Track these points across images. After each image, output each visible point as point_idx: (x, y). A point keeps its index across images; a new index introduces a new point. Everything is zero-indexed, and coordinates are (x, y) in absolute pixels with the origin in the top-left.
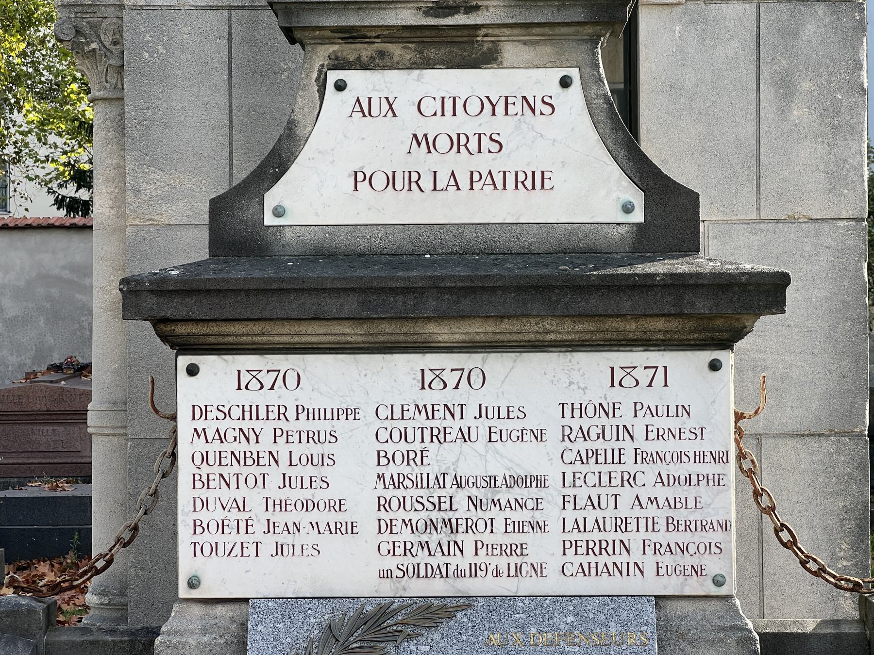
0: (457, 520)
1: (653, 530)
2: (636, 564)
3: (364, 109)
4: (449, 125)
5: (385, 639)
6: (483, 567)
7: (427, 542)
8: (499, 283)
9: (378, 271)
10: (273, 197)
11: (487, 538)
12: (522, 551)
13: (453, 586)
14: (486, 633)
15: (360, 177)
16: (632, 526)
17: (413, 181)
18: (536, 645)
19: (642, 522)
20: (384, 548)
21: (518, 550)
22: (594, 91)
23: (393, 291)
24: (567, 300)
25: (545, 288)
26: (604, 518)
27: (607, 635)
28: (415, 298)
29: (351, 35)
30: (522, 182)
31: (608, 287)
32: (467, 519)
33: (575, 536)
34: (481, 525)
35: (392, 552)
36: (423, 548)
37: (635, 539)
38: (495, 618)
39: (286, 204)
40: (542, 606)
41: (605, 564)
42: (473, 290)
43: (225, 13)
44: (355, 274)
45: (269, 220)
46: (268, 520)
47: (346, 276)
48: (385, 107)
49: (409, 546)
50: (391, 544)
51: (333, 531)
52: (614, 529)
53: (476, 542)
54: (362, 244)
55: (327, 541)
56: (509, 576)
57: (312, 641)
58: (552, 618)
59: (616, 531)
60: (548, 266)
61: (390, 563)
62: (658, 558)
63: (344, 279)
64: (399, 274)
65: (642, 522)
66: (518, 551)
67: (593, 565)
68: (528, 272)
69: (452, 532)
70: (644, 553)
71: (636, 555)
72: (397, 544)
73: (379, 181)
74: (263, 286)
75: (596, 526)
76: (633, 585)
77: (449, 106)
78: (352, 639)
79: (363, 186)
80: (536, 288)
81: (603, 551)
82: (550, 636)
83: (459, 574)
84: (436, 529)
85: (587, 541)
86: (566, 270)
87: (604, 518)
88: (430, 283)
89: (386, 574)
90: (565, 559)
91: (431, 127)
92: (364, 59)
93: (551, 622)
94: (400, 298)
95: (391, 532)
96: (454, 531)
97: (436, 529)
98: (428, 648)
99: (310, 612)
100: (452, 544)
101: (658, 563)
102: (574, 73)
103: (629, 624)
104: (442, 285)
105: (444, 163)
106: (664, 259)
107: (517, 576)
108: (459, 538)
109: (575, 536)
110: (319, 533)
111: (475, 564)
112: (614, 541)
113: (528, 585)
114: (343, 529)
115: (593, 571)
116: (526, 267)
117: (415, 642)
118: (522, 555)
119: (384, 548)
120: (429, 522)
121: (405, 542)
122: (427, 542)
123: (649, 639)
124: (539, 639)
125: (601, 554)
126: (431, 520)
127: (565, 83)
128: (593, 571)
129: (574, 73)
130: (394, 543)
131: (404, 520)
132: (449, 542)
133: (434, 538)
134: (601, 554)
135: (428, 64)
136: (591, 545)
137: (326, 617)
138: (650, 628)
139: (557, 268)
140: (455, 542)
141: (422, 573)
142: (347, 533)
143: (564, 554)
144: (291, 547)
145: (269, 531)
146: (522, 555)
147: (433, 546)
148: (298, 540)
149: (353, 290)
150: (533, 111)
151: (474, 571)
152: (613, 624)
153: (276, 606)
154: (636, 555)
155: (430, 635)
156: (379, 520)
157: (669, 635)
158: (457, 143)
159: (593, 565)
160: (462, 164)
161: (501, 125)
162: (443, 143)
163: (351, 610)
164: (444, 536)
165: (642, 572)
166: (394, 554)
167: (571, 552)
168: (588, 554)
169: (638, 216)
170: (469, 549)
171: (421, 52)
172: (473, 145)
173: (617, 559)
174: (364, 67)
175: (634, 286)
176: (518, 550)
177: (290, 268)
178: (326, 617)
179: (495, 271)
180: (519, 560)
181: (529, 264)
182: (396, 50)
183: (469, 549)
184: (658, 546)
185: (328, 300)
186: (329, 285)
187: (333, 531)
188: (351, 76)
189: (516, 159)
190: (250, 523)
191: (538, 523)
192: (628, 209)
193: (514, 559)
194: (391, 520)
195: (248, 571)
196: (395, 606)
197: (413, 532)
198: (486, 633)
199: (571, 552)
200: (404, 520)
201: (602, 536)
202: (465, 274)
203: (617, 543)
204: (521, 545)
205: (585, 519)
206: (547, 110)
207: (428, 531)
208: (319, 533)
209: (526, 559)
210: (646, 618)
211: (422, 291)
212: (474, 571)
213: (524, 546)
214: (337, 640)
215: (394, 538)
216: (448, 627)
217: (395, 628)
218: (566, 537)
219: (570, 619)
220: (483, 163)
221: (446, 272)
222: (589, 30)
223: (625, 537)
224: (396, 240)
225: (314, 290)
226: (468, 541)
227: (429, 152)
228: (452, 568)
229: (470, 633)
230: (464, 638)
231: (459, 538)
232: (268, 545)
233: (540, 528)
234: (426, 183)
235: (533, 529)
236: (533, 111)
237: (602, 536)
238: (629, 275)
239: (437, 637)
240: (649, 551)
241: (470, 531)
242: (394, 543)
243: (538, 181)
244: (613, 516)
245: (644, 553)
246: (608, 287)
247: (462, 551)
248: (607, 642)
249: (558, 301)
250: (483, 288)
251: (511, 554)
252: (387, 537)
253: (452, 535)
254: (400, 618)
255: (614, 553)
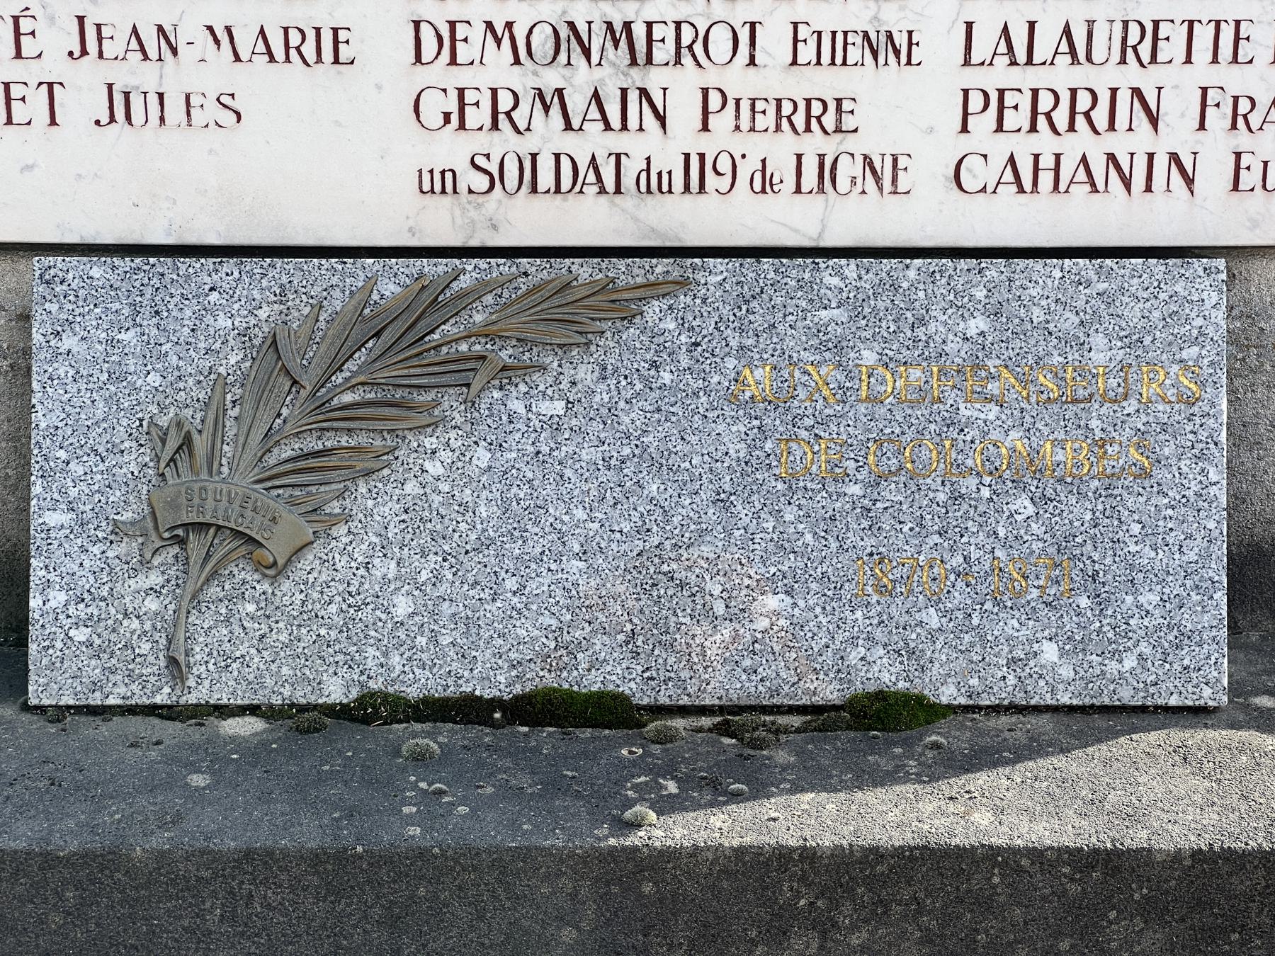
0: (649, 25)
1: (1235, 59)
2: (1175, 158)
5: (433, 380)
6: (724, 165)
7: (559, 92)
11: (738, 81)
12: (839, 121)
13: (636, 220)
14: (731, 363)
16: (1173, 49)
18: (875, 400)
19: (1204, 36)
20: (434, 106)
21: (830, 115)
26: (1090, 23)
27: (1081, 371)
32: (678, 25)
33: (1000, 75)
34: (720, 42)
35: (455, 118)
36: (546, 108)
37: (1176, 86)
38: (759, 321)
40: (895, 287)
41: (1084, 160)
46: (81, 19)
49: (505, 102)
50: (453, 95)
51: (279, 53)
52: (1116, 56)
53: (705, 92)
55: (258, 83)
56: (798, 190)
57: (222, 383)
58: (922, 322)
59: (1123, 61)
61: (452, 150)
62: (1242, 139)
65: (1204, 36)
66: (829, 121)
67: (1047, 162)
69: (634, 62)
70: (1202, 127)
71: (1178, 133)
72: (470, 97)
75: (1064, 47)
76: (1162, 217)
78: (339, 378)
81: (1080, 120)
82: (916, 373)
83: (653, 183)
84: (587, 53)
85: (1035, 92)
87: (1090, 23)
89: (440, 183)
90: (966, 144)
93: (920, 332)
95: (453, 61)
96: (642, 58)
97: (587, 53)
98: (559, 407)
99: (214, 296)
100: (633, 96)
101: (1238, 155)
103: (1147, 340)
107: (821, 190)
108: (655, 80)
109: (1000, 75)
110: (237, 58)
111: (702, 156)
112: (1114, 91)
113: (854, 218)
114: (309, 50)
115: (1046, 179)
117: (523, 388)
118: (838, 130)
119: (434, 106)
120: (564, 32)
121: (494, 92)
122: (559, 92)
123: (1203, 385)
124: (883, 382)
125: (1072, 128)
126: (571, 25)
128: (1046, 179)
130: (461, 92)
131: (489, 25)
132: (624, 91)
133: (579, 80)
134: (1072, 128)
136: (1045, 102)
137: (263, 314)
138: (1209, 353)
140: (644, 92)
141: (546, 179)
142: (319, 59)
143: (965, 129)
144: (153, 100)
145: (84, 52)
146: (838, 130)
147: (577, 102)
148: (176, 78)
151: (696, 175)
152: (1099, 340)
153: (114, 279)
154: (1178, 133)
155: (568, 371)
156: (417, 24)
157: (1253, 361)
159: (1047, 162)
163: (337, 293)
164: (610, 74)
165: (1189, 182)
166: (462, 126)
167: (983, 123)
168: (1033, 129)
170: (684, 111)
173: (1120, 144)
176: (830, 115)
178: (263, 314)
180: (830, 146)
183: (684, 111)
184: (1244, 106)
187: (279, 53)
190: (25, 25)
191: (890, 36)
193: (814, 144)
194: (452, 25)
195: (28, 168)
196: (464, 282)
197: (517, 61)
198: (731, 363)
199: (983, 123)
200: (489, 25)
201: (1081, 76)
203: (1124, 98)
204: (839, 101)
205: (1032, 25)
207: (563, 57)
208: (237, 58)
209: (851, 143)
210: (1199, 322)
212: (696, 175)
213: (847, 106)
214: (295, 382)
215: (462, 77)
216: (621, 345)
217: (463, 347)
218: (974, 78)
219: (977, 324)
223: (1147, 81)
226: (679, 87)
228: (631, 168)
229: (684, 364)
230: (666, 377)
231: (655, 80)
232: (84, 92)
233: (897, 53)
235: (875, 54)
237: (1081, 76)
239: (586, 373)
240: (1218, 119)
241: (687, 59)
242: (461, 92)
244: (1119, 18)
245: (1202, 127)
247: (661, 119)
248: (1081, 393)
251: (808, 129)
252: (439, 74)
253: (634, 72)
254: (478, 318)
255: (1112, 126)
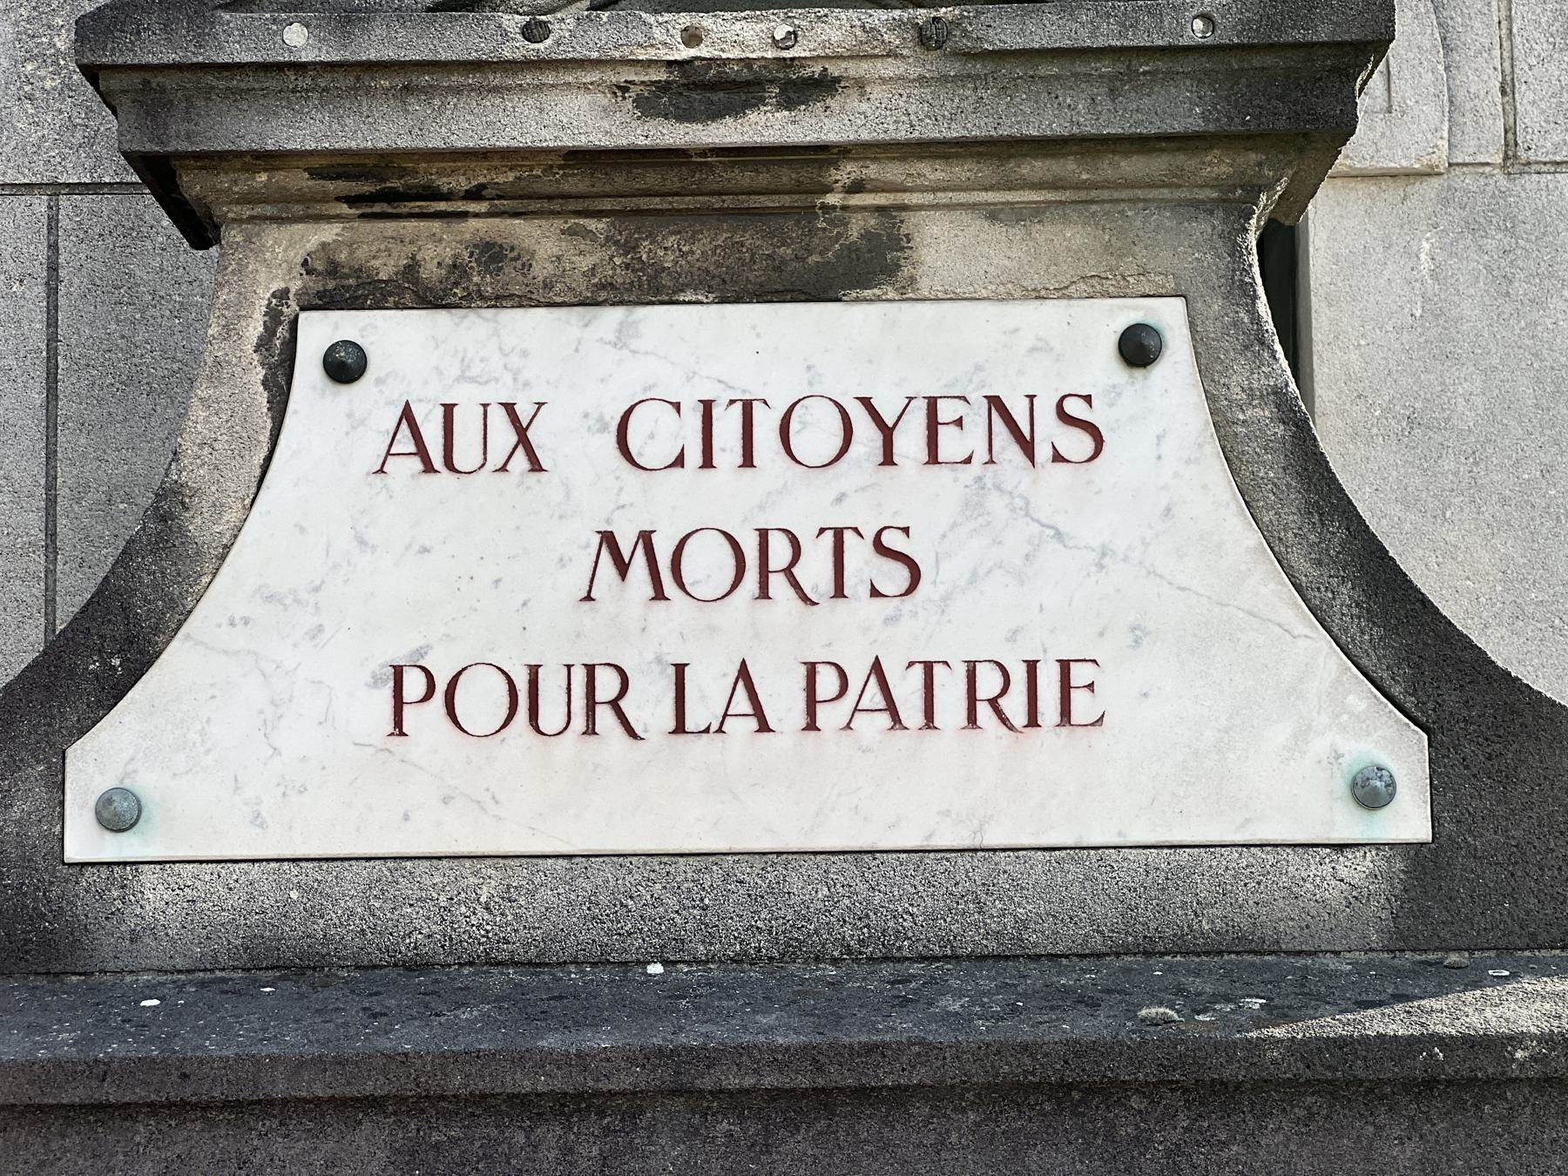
3: (426, 445)
4: (732, 499)
8: (920, 1075)
9: (469, 1028)
10: (97, 760)
15: (414, 685)
17: (601, 701)
22: (1239, 378)
23: (525, 1106)
24: (1175, 1136)
25: (1090, 1090)
28: (607, 1131)
29: (384, 186)
30: (993, 702)
31: (1331, 1089)
39: (146, 784)
42: (823, 1099)
43: (40, 204)
44: (384, 1044)
45: (83, 841)
47: (349, 1052)
48: (503, 436)
54: (419, 927)
60: (1094, 1004)
63: (340, 1062)
64: (551, 1041)
68: (1025, 1032)
73: (482, 700)
74: (31, 1094)
77: (731, 431)
79: (425, 719)
80: (1060, 1091)
86: (1168, 1021)
88: (664, 1075)
91: (666, 507)
92: (430, 271)
94: (550, 1134)
102: (1169, 316)
104: (707, 1083)
105: (713, 633)
106: (1514, 976)
116: (1014, 1010)
127: (1138, 349)
129: (1169, 316)
135: (653, 288)
139: (1131, 1013)
149: (373, 1103)
150: (1027, 447)
158: (758, 564)
160: (777, 638)
161: (917, 499)
162: (707, 564)
169: (1409, 820)
171: (629, 248)
172: (815, 570)
174: (431, 299)
175: (1430, 1083)
177: (143, 1023)
179: (902, 1027)
181: (1024, 996)
182: (541, 240)
185: (279, 1145)
186: (280, 1090)
188: (385, 333)
189: (966, 622)
192: (1371, 793)
202: (793, 1039)
206: (1076, 444)
211: (632, 1104)
220: (852, 634)
221: (721, 1034)
222: (1218, 165)
224: (543, 914)
225: (226, 1105)
227: (659, 595)
234: (650, 705)
236: (1027, 447)
238: (1411, 1041)
243: (1045, 695)
246: (1331, 1089)
249: (1142, 1141)
250: (862, 1094)
